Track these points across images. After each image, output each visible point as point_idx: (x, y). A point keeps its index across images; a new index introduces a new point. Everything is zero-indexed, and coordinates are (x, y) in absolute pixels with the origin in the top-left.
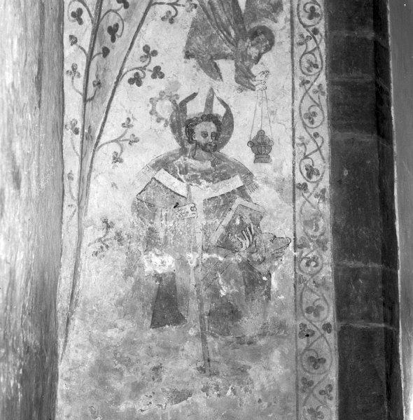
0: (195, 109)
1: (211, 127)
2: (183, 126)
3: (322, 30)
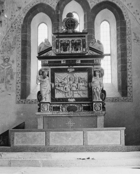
0: (5, 58)
1: (7, 60)
2: (4, 60)
3: (20, 46)
